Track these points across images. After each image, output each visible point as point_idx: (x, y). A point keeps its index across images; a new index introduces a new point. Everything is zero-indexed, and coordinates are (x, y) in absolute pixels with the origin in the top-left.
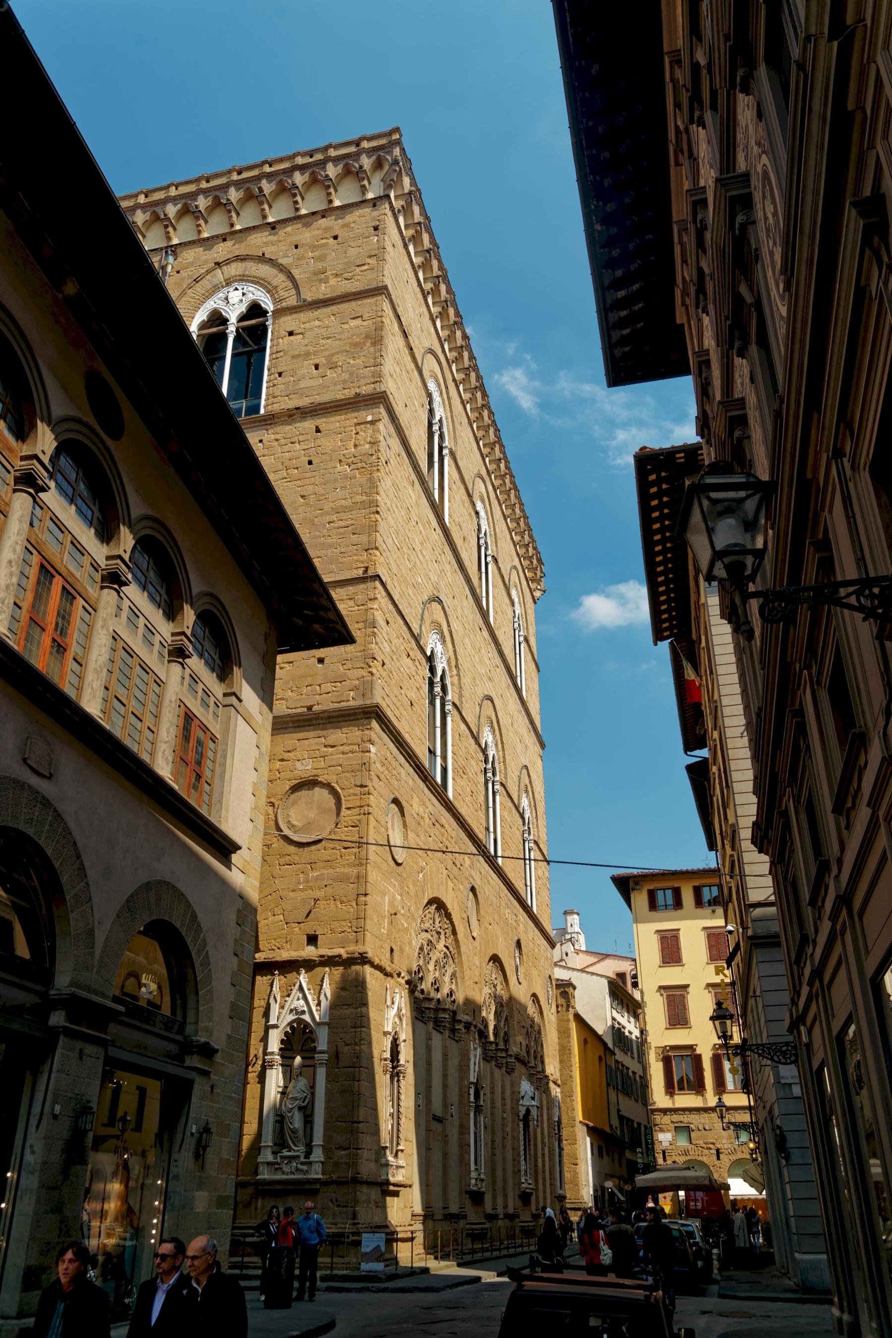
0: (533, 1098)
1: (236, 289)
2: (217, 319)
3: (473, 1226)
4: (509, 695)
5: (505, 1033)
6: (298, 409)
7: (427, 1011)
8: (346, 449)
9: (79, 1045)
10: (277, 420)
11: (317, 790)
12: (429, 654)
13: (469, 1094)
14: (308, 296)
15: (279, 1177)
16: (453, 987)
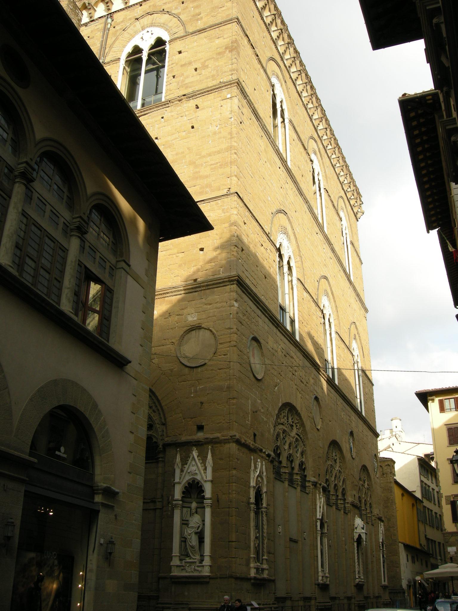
0: (363, 528)
2: (137, 50)
3: (326, 604)
4: (340, 277)
5: (343, 489)
6: (184, 95)
7: (284, 474)
8: (215, 116)
11: (202, 332)
12: (278, 247)
13: (317, 526)
14: (191, 29)
15: (184, 574)
16: (304, 460)
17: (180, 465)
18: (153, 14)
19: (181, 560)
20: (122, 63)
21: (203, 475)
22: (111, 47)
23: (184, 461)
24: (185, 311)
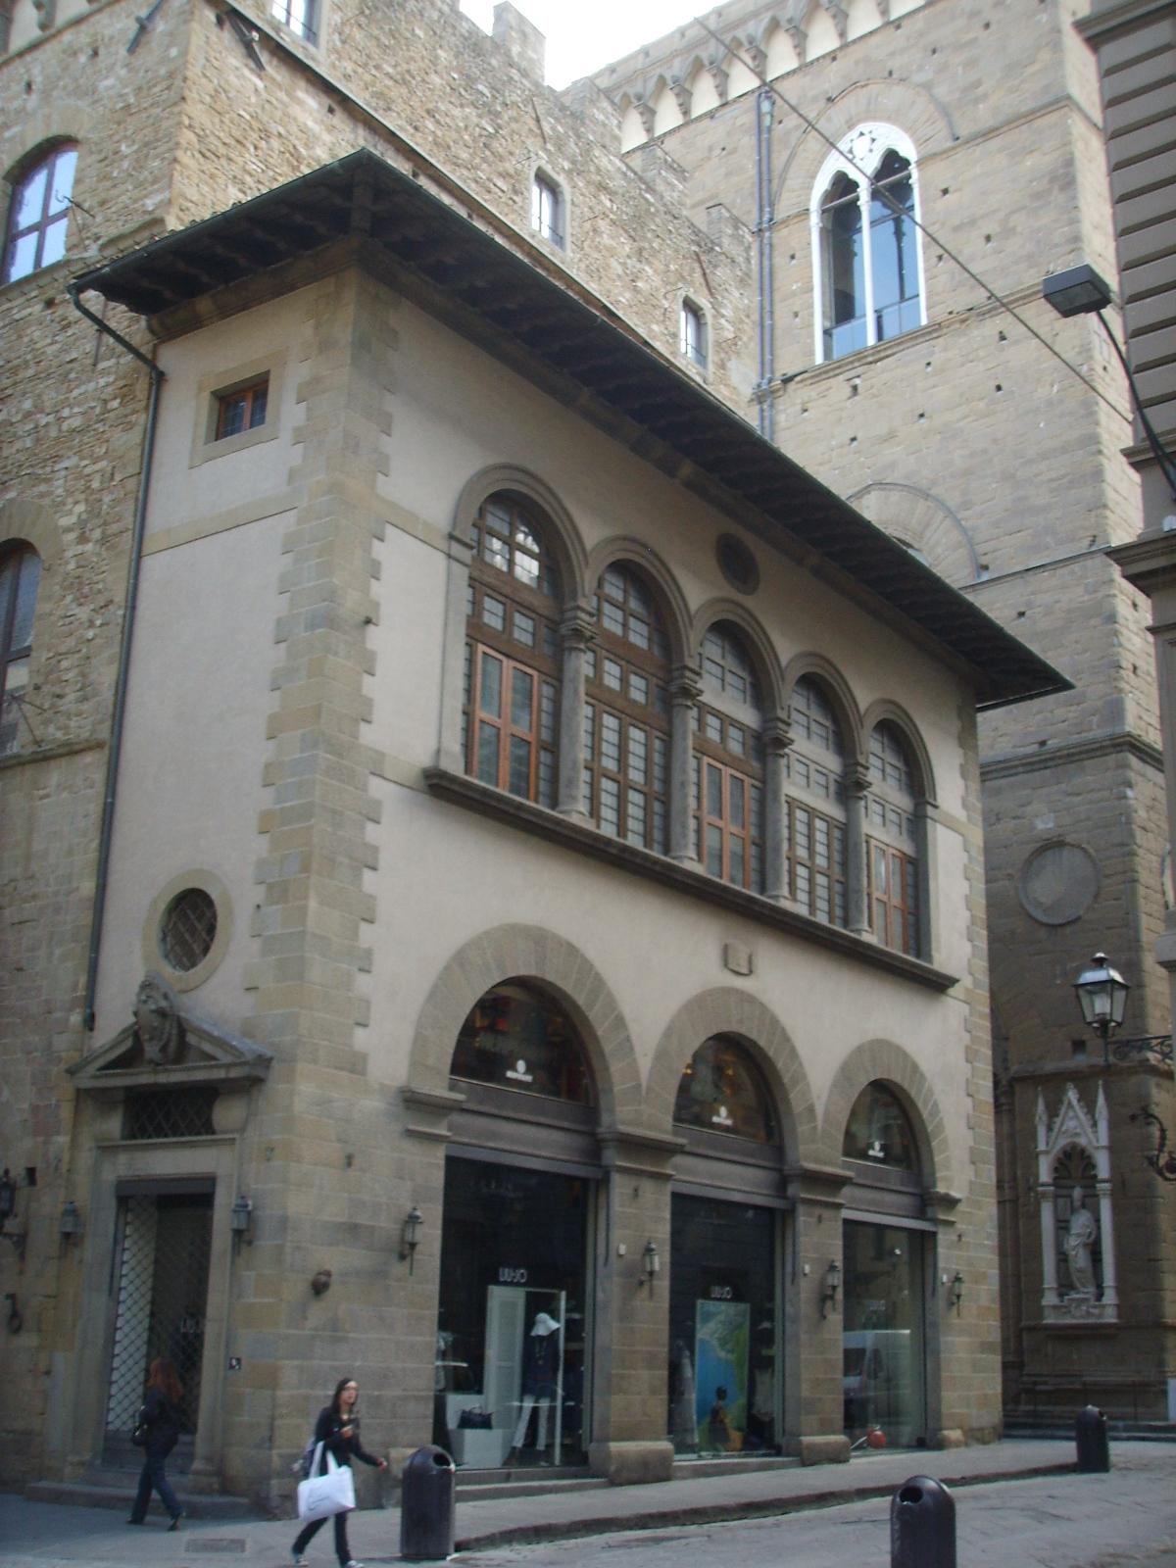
1: (862, 134)
2: (843, 185)
9: (817, 1211)
10: (945, 331)
11: (1066, 852)
14: (965, 129)
15: (1068, 1321)
17: (1045, 1118)
18: (866, 85)
19: (1061, 1295)
20: (815, 220)
21: (1091, 1136)
22: (783, 179)
23: (1053, 1111)
24: (1029, 809)
